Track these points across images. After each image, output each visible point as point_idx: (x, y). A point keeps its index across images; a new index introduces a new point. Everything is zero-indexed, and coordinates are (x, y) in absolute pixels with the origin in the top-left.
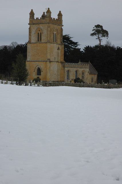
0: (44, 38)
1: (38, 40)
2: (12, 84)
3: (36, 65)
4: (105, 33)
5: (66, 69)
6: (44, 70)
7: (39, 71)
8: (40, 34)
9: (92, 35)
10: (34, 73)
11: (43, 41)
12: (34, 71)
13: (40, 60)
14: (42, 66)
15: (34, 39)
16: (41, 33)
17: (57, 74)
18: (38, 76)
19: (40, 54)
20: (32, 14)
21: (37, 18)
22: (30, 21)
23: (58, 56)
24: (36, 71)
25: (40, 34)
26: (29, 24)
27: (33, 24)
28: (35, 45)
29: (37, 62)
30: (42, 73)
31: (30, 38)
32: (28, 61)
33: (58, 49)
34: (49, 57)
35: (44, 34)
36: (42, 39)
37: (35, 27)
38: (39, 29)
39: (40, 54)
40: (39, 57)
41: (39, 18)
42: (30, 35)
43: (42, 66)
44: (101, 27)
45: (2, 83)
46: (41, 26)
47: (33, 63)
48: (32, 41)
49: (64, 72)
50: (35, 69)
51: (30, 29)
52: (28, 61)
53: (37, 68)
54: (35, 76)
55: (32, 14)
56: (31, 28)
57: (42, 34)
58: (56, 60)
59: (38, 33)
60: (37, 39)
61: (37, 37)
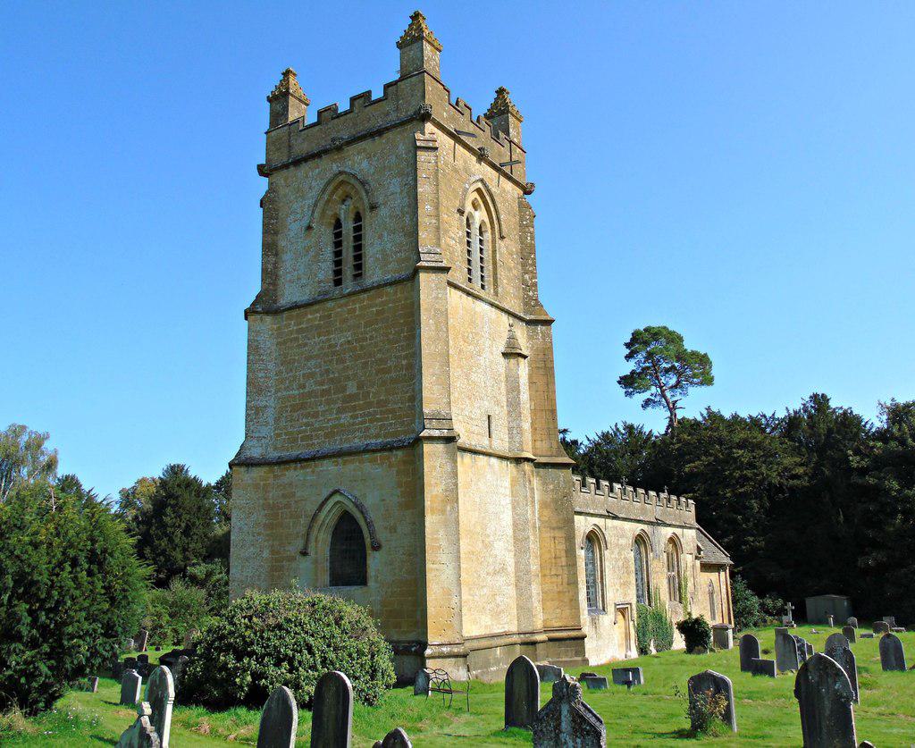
1: (338, 273)
4: (696, 368)
5: (583, 525)
6: (393, 530)
8: (348, 227)
10: (305, 564)
11: (374, 274)
12: (300, 544)
13: (357, 442)
14: (369, 502)
16: (358, 218)
17: (511, 569)
19: (352, 388)
20: (280, 98)
21: (328, 115)
23: (514, 405)
24: (322, 543)
25: (348, 227)
26: (262, 170)
28: (313, 316)
29: (329, 467)
30: (375, 562)
33: (511, 354)
35: (383, 211)
36: (371, 251)
37: (313, 178)
38: (345, 186)
39: (352, 388)
40: (345, 419)
44: (674, 339)
46: (358, 161)
47: (293, 474)
48: (290, 293)
49: (571, 553)
50: (310, 527)
51: (268, 203)
53: (329, 517)
55: (280, 98)
56: (282, 191)
57: (367, 222)
58: (501, 443)
59: (338, 224)
60: (325, 270)
61: (329, 251)
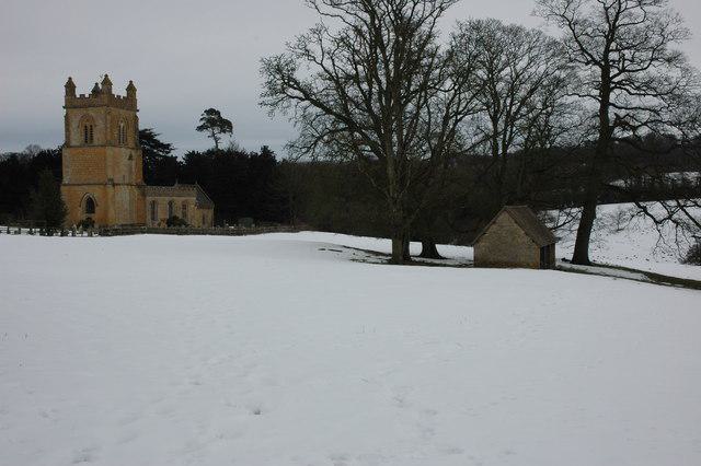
0: (98, 137)
2: (30, 233)
3: (82, 193)
4: (226, 126)
5: (149, 199)
7: (91, 205)
9: (200, 128)
11: (96, 142)
15: (77, 139)
18: (89, 215)
20: (70, 86)
22: (66, 101)
23: (131, 172)
24: (84, 204)
27: (75, 107)
30: (97, 209)
31: (67, 137)
32: (65, 185)
33: (130, 158)
34: (110, 175)
36: (95, 137)
37: (77, 115)
41: (87, 96)
42: (67, 130)
43: (96, 193)
44: (218, 113)
45: (8, 232)
46: (92, 112)
47: (76, 188)
48: (73, 143)
51: (67, 117)
52: (65, 185)
54: (81, 215)
55: (70, 86)
58: (127, 181)
